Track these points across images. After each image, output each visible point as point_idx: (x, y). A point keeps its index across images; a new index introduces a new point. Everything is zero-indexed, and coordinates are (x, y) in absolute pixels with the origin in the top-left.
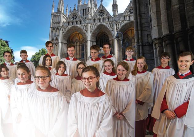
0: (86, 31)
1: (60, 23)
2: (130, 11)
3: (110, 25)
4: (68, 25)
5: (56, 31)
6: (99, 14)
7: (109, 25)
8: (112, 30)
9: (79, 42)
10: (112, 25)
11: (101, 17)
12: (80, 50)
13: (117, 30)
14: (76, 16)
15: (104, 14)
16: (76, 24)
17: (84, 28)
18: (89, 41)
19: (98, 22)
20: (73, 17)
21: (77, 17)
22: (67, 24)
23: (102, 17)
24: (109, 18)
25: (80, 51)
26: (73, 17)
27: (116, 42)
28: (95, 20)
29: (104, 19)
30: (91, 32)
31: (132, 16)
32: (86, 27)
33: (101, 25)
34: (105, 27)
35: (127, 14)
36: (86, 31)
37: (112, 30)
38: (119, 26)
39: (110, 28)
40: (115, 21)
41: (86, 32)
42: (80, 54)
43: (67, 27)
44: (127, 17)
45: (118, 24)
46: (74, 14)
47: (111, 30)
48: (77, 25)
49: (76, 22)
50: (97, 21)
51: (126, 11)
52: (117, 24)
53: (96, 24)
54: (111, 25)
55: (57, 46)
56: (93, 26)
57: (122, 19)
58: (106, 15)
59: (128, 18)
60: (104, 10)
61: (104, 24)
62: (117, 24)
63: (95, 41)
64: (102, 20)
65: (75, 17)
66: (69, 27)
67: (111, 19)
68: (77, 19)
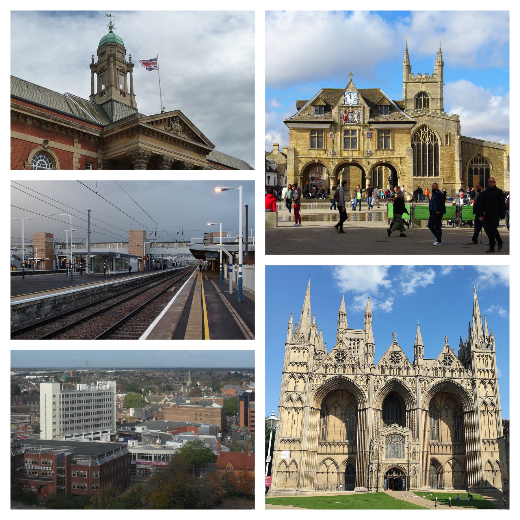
2: (444, 361)
4: (326, 372)
6: (390, 359)
11: (393, 365)
13: (423, 393)
14: (343, 354)
15: (399, 359)
16: (344, 372)
20: (336, 358)
21: (345, 358)
22: (325, 369)
23: (397, 365)
24: (408, 369)
26: (336, 358)
29: (399, 368)
31: (448, 371)
35: (439, 366)
37: (414, 393)
38: (427, 386)
39: (411, 389)
40: (420, 376)
41: (366, 391)
43: (325, 376)
45: (425, 383)
46: (339, 351)
48: (347, 376)
49: (345, 367)
50: (387, 372)
53: (386, 376)
56: (380, 381)
57: (431, 373)
59: (440, 373)
61: (400, 379)
62: (423, 382)
65: (340, 358)
66: (329, 377)
68: (346, 362)
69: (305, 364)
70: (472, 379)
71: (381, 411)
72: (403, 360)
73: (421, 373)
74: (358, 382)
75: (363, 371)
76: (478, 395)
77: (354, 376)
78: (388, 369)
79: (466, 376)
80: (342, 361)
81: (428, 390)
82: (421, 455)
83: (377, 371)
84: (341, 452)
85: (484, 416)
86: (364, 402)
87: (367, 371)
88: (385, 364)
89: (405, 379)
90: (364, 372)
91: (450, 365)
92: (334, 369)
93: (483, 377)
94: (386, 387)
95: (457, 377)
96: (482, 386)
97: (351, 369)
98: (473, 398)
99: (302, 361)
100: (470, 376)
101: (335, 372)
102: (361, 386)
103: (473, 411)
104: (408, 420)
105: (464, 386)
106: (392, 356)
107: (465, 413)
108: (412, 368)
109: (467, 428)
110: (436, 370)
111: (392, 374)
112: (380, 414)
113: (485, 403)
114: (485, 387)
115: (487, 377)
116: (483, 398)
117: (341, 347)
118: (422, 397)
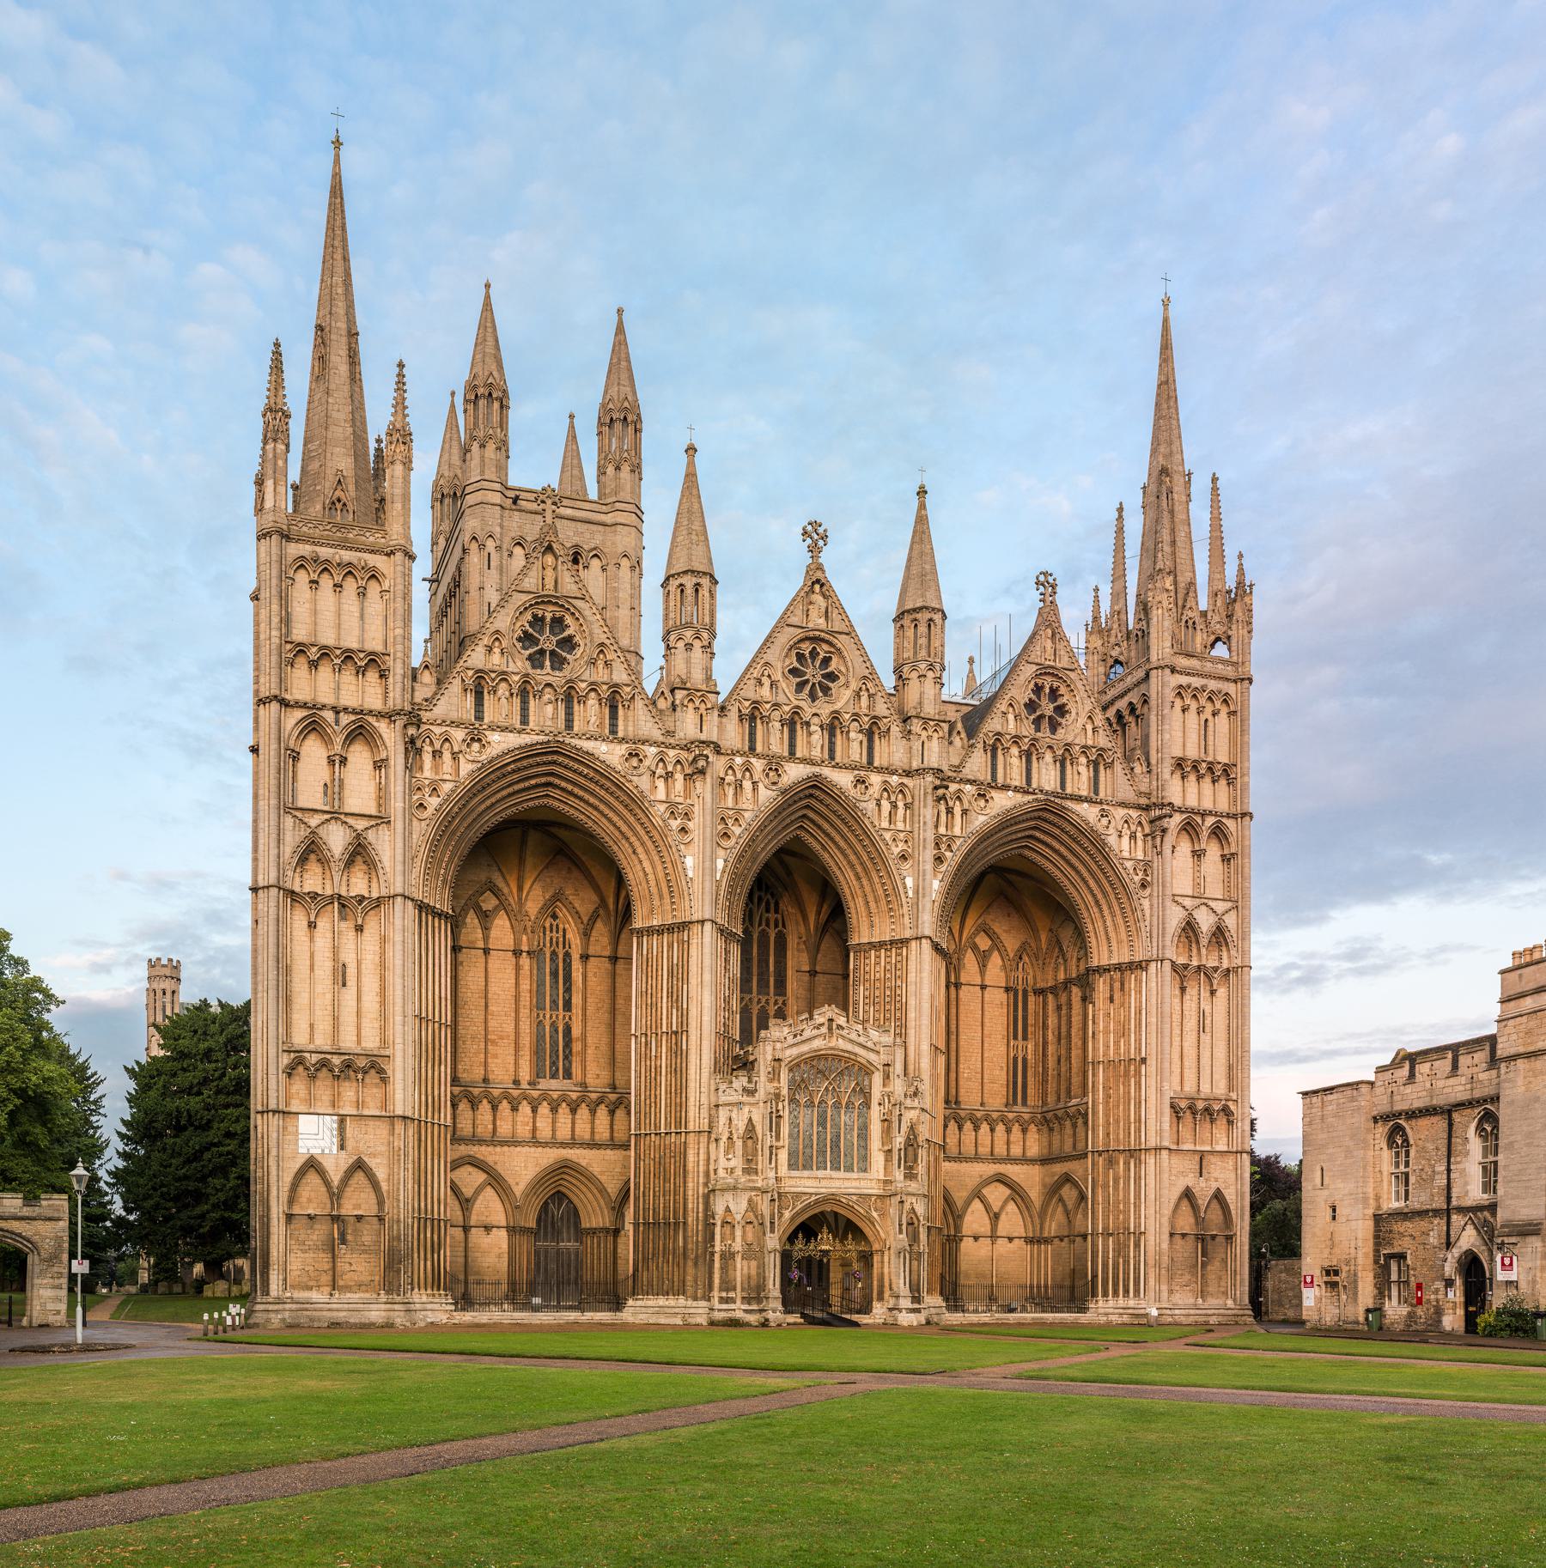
0: (675, 824)
2: (1031, 706)
3: (886, 805)
6: (794, 672)
8: (904, 857)
10: (900, 804)
13: (939, 859)
14: (558, 622)
15: (832, 677)
17: (660, 784)
19: (786, 754)
20: (527, 639)
21: (569, 643)
28: (752, 717)
29: (832, 727)
31: (1048, 757)
32: (679, 777)
33: (815, 788)
34: (844, 814)
36: (675, 824)
37: (904, 857)
38: (957, 831)
39: (888, 836)
41: (683, 830)
44: (1015, 751)
45: (949, 811)
47: (896, 851)
48: (588, 745)
49: (570, 697)
50: (774, 739)
53: (774, 765)
54: (894, 806)
55: (359, 929)
56: (747, 785)
57: (977, 765)
58: (858, 695)
60: (842, 642)
61: (843, 779)
62: (943, 807)
64: (813, 743)
65: (548, 641)
66: (499, 743)
67: (893, 751)
70: (1147, 808)
72: (854, 685)
74: (644, 782)
75: (670, 725)
76: (1168, 892)
77: (622, 750)
79: (1126, 792)
80: (558, 662)
81: (961, 847)
83: (732, 734)
84: (524, 1131)
85: (1183, 990)
86: (673, 887)
87: (688, 725)
88: (765, 692)
89: (860, 781)
91: (1054, 727)
92: (517, 701)
93: (1192, 802)
94: (777, 812)
95: (1084, 793)
96: (1185, 847)
97: (607, 711)
98: (1146, 903)
100: (1140, 794)
103: (1141, 966)
105: (1112, 840)
106: (800, 657)
107: (1102, 970)
108: (895, 730)
109: (1103, 1045)
113: (1189, 929)
114: (1198, 855)
115: (1207, 804)
116: (1188, 902)
118: (936, 884)
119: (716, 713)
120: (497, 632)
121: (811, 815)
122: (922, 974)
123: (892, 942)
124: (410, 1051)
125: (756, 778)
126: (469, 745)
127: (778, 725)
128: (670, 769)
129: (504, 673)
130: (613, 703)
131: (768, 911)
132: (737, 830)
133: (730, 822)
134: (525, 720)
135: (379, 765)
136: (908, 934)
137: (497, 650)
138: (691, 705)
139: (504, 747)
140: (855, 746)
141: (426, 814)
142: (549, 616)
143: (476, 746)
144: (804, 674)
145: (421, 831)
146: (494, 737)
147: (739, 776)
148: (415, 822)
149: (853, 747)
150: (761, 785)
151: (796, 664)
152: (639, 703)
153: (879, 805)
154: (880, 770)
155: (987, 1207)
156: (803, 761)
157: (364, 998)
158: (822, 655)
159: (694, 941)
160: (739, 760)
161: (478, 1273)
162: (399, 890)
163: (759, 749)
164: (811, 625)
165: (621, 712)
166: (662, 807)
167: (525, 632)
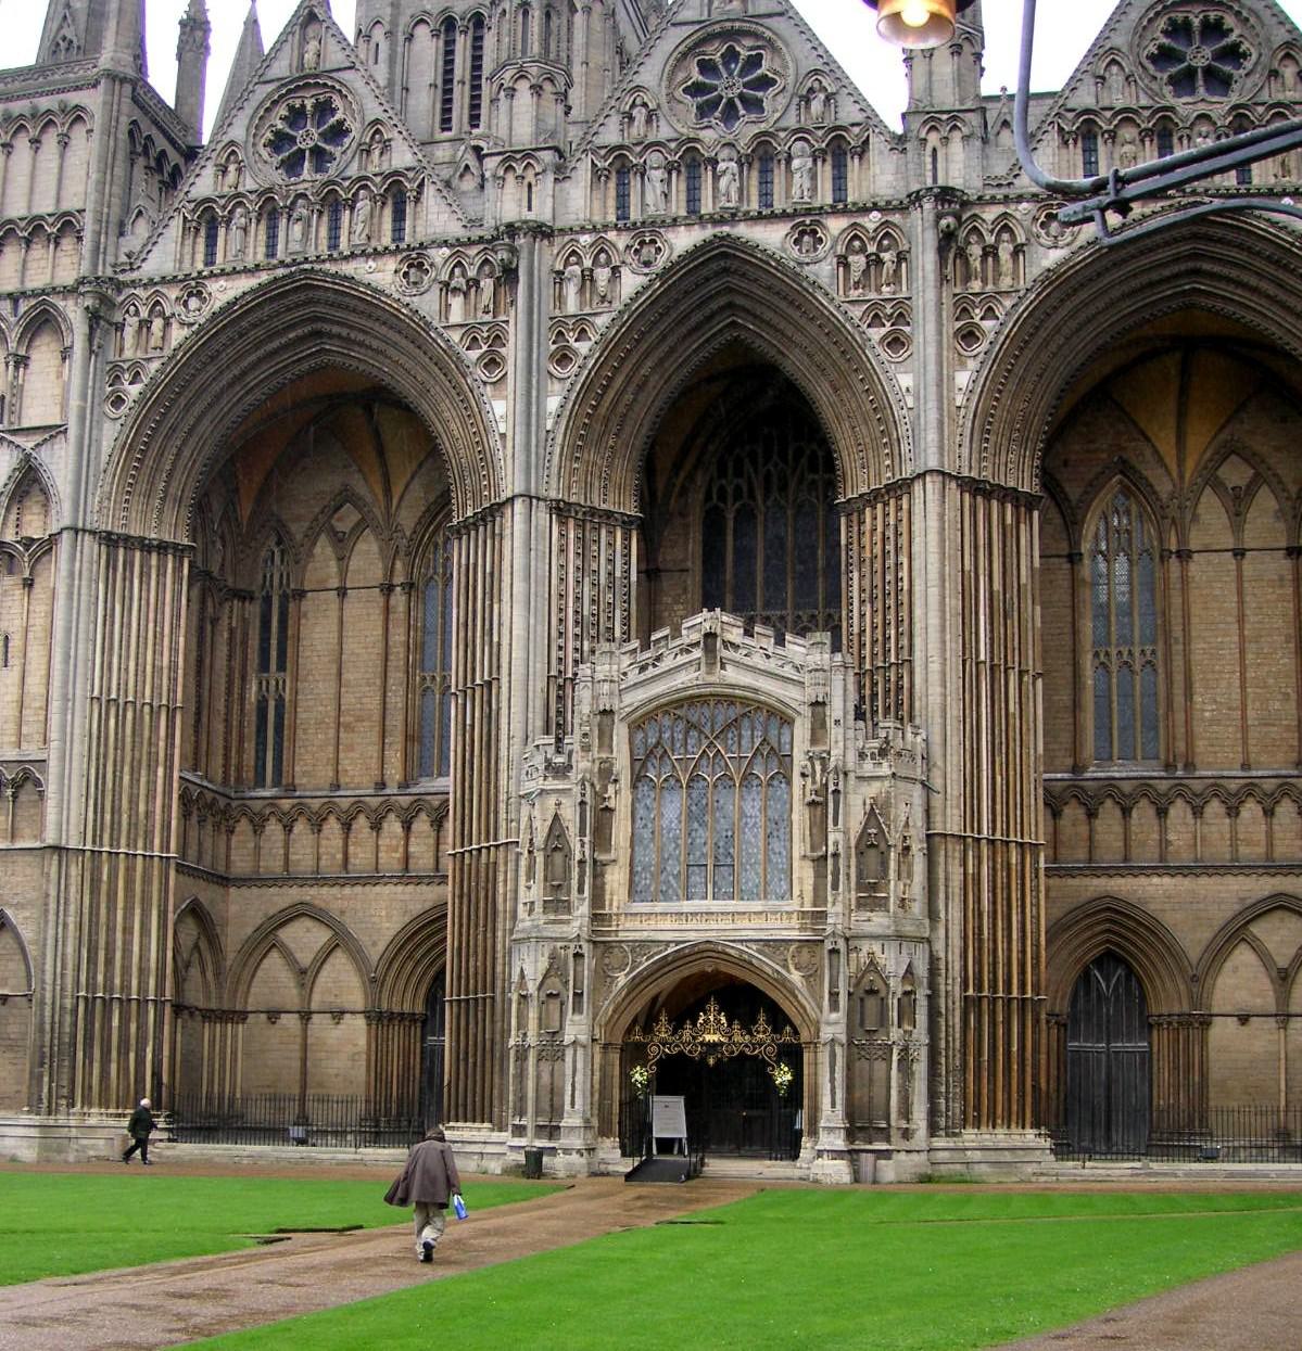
1: (80, 239)
3: (857, 262)
4: (210, 261)
5: (21, 362)
6: (696, 90)
7: (843, 262)
9: (387, 531)
12: (398, 652)
14: (324, 109)
15: (765, 83)
16: (334, 242)
18: (519, 505)
20: (279, 141)
21: (338, 133)
23: (746, 130)
25: (396, 677)
26: (279, 141)
27: (930, 533)
30: (563, 358)
32: (487, 284)
34: (781, 290)
42: (396, 721)
43: (194, 287)
48: (347, 268)
49: (333, 203)
51: (1102, 57)
52: (976, 250)
53: (647, 233)
55: (29, 584)
56: (603, 275)
61: (771, 237)
63: (631, 509)
64: (724, 188)
65: (309, 136)
66: (223, 292)
68: (346, 164)
69: (68, 224)
71: (627, 523)
73: (959, 167)
74: (427, 304)
75: (473, 208)
78: (670, 168)
82: (952, 871)
83: (580, 200)
87: (507, 204)
90: (476, 222)
97: (388, 212)
99: (45, 206)
101: (271, 252)
102: (455, 336)
104: (854, 585)
106: (707, 67)
110: (1086, 131)
111: (707, 207)
112: (619, 555)
117: (309, 57)
119: (550, 177)
120: (232, 143)
121: (740, 301)
122: (930, 533)
123: (889, 488)
124: (79, 748)
125: (616, 261)
126: (185, 304)
127: (657, 175)
128: (472, 273)
129: (239, 195)
130: (398, 194)
131: (722, 473)
132: (583, 348)
133: (571, 337)
134: (271, 252)
135: (66, 354)
136: (908, 471)
137: (232, 168)
138: (510, 177)
139: (230, 295)
140: (800, 181)
141: (124, 410)
142: (309, 104)
143: (194, 303)
144: (715, 88)
145: (110, 435)
146: (222, 282)
147: (588, 263)
148: (107, 425)
149: (803, 181)
150: (625, 271)
151: (696, 76)
152: (429, 192)
153: (847, 266)
154: (845, 212)
155: (1264, 956)
156: (702, 221)
157: (29, 680)
158: (744, 53)
159: (507, 532)
160: (586, 239)
161: (320, 1085)
162: (66, 522)
163: (635, 215)
164: (715, 16)
165: (409, 209)
166: (455, 336)
167: (279, 134)
